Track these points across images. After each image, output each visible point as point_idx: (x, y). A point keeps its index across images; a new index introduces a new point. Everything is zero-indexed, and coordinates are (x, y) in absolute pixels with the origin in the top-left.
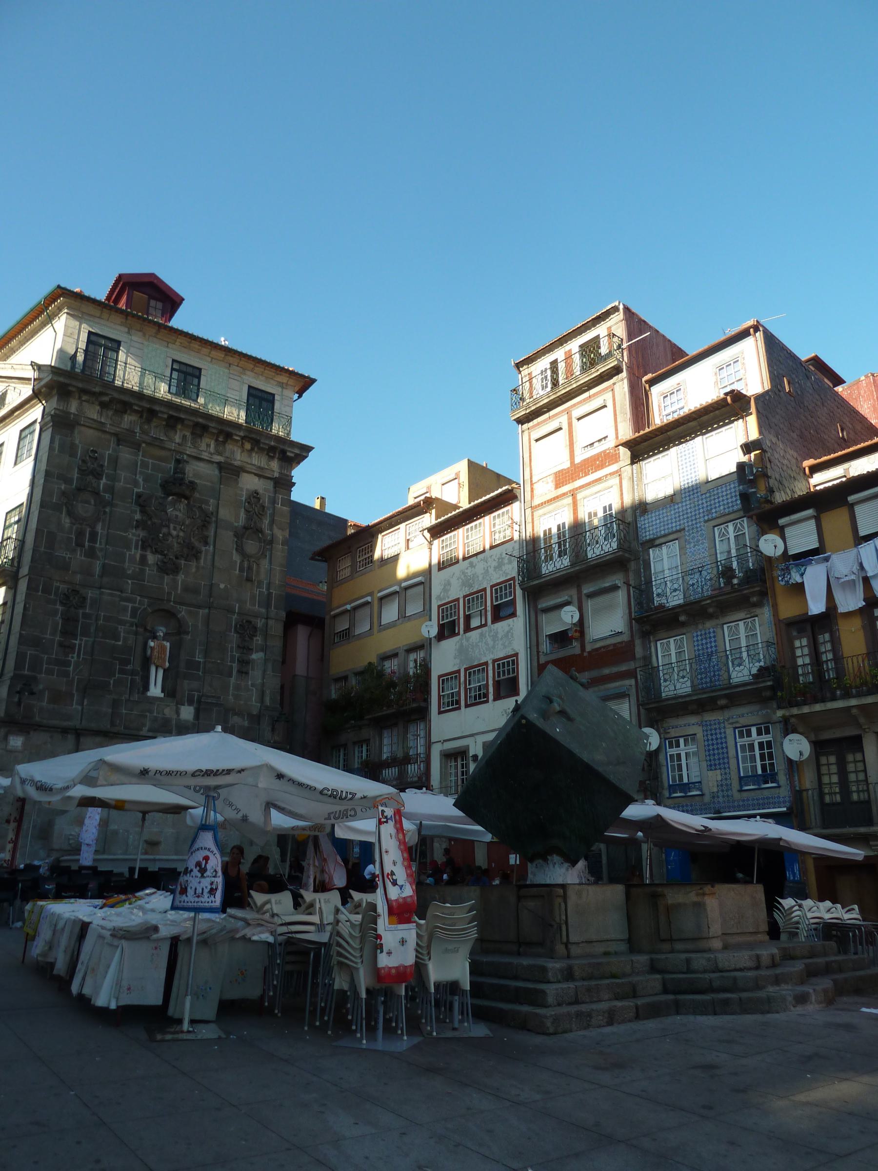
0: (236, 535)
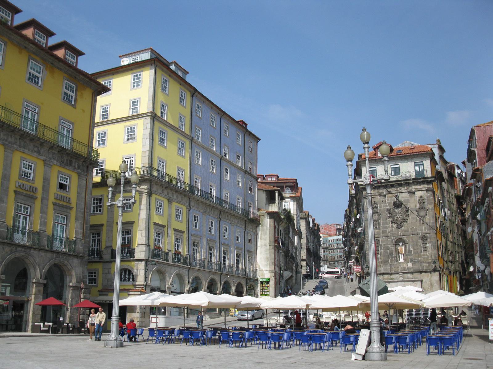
0: (417, 211)
